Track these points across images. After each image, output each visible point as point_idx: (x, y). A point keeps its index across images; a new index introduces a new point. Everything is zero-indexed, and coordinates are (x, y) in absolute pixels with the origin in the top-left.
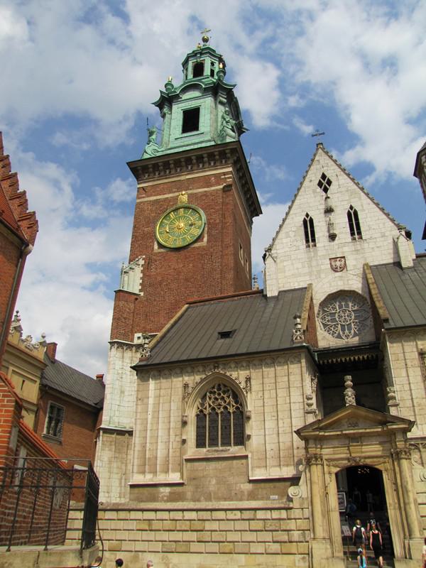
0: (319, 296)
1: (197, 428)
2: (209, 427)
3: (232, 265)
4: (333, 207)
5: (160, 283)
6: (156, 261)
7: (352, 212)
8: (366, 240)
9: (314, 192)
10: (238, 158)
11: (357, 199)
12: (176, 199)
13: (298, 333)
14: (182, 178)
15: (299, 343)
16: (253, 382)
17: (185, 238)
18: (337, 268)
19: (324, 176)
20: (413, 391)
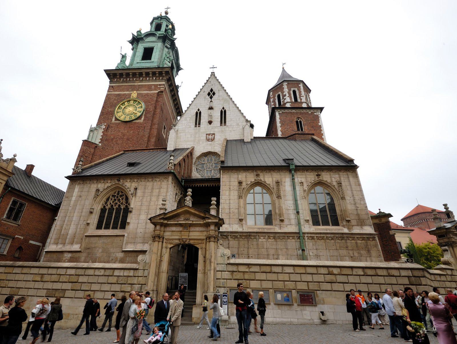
0: (197, 153)
1: (100, 217)
2: (107, 216)
3: (155, 134)
4: (214, 107)
5: (112, 140)
6: (112, 127)
7: (223, 111)
8: (228, 126)
9: (205, 98)
10: (170, 78)
11: (227, 104)
12: (130, 95)
13: (170, 165)
14: (136, 84)
15: (169, 170)
16: (138, 191)
17: (131, 116)
18: (209, 139)
19: (212, 90)
20: (231, 204)
